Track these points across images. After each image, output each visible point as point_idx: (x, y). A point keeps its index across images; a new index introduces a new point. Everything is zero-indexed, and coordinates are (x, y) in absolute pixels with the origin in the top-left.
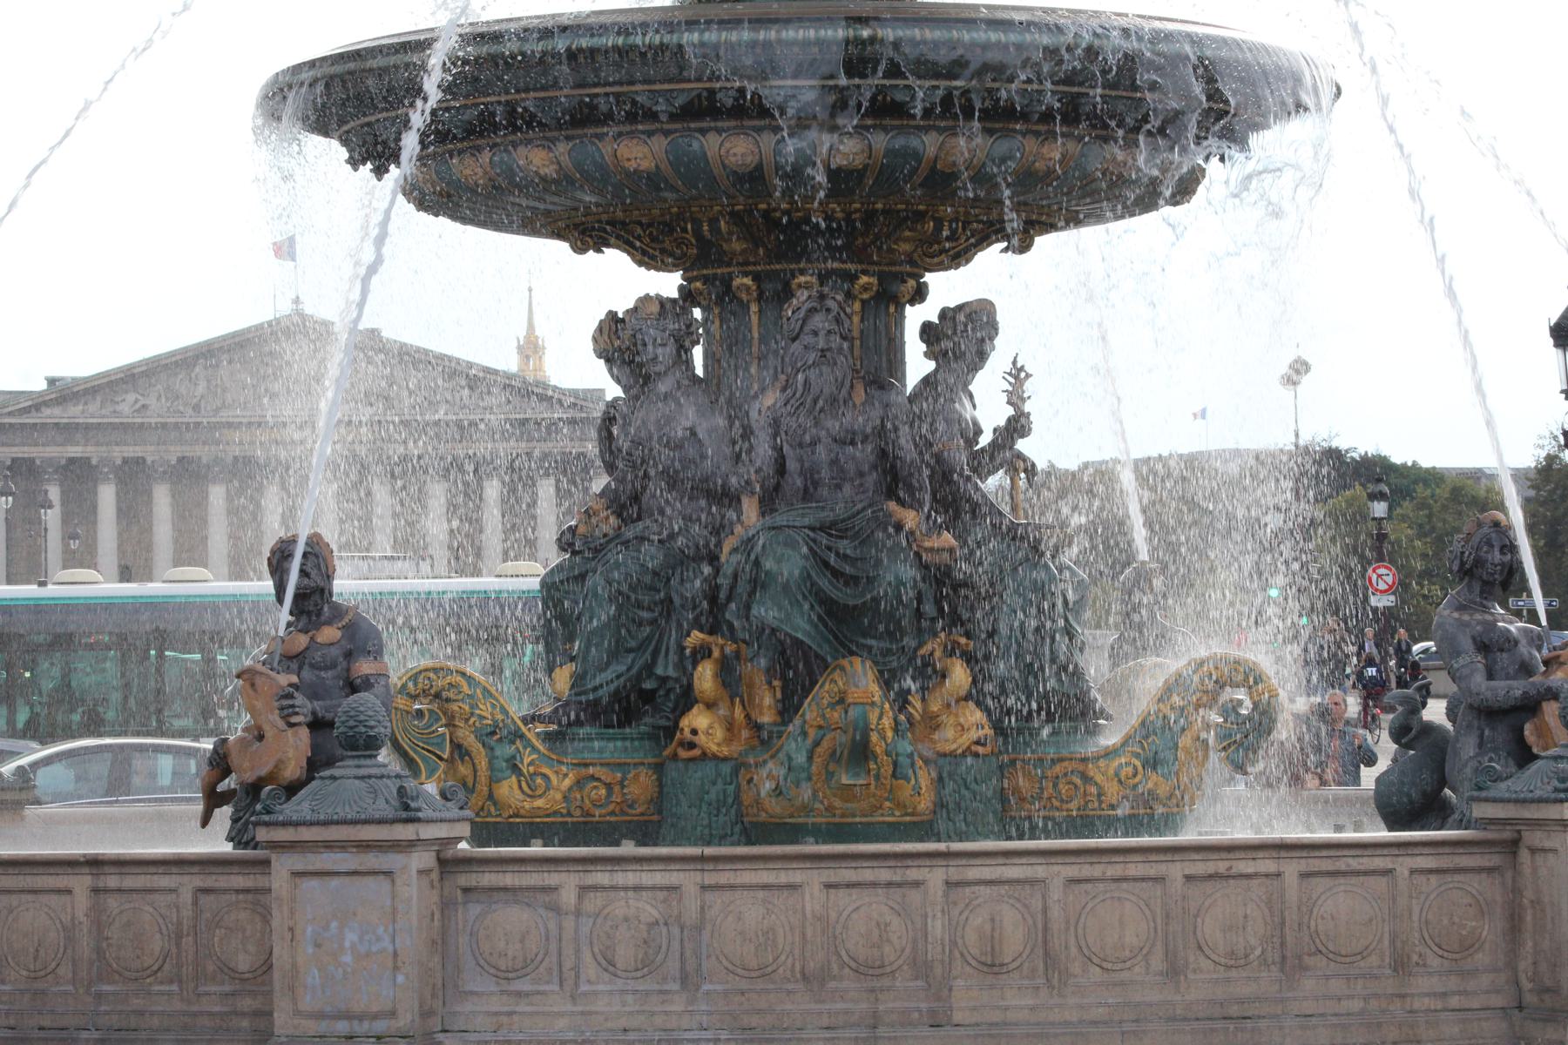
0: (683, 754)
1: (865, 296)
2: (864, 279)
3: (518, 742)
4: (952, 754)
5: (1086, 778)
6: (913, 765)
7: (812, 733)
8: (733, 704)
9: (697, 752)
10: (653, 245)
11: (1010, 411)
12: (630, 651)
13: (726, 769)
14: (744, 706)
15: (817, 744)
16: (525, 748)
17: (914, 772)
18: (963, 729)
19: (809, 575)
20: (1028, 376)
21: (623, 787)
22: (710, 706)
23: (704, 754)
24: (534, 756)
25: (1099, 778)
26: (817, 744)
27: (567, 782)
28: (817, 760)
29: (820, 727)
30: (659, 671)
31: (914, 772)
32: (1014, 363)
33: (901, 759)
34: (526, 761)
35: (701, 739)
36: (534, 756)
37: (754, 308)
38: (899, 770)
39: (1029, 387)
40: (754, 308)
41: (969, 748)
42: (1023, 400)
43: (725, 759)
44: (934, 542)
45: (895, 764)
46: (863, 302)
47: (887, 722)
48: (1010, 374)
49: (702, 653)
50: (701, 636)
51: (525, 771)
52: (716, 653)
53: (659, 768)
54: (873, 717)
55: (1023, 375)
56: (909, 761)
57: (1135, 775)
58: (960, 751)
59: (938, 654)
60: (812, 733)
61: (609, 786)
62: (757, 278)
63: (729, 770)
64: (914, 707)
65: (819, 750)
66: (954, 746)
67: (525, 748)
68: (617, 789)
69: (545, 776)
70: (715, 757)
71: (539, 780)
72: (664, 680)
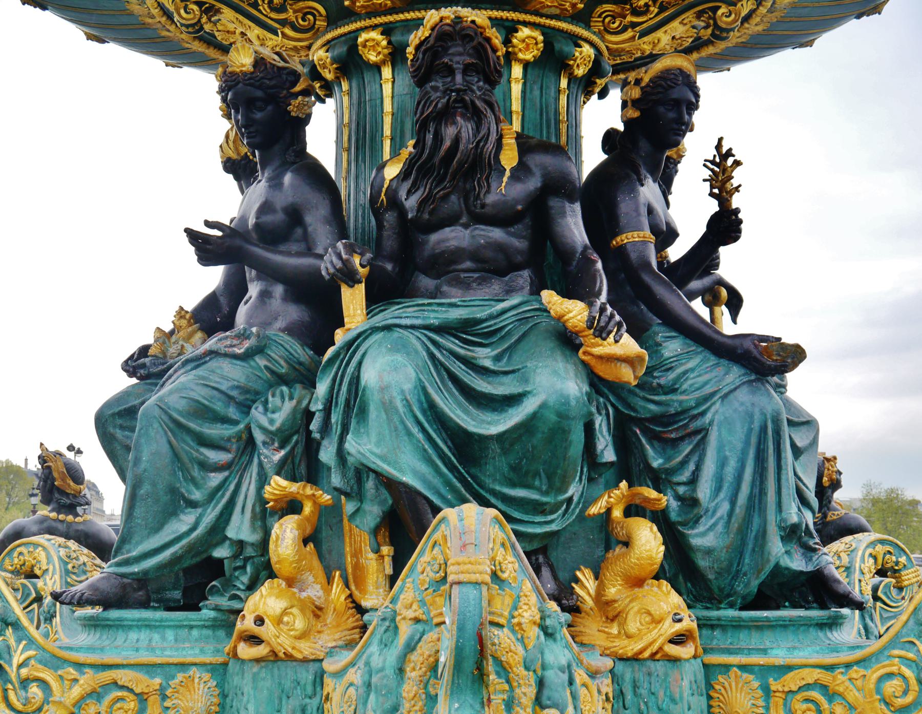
0: (246, 651)
1: (529, 56)
2: (525, 32)
3: (9, 631)
4: (635, 659)
5: (831, 694)
6: (571, 682)
7: (406, 630)
8: (330, 580)
9: (261, 651)
10: (273, 15)
11: (713, 206)
12: (193, 504)
13: (306, 675)
14: (347, 586)
15: (410, 647)
16: (19, 641)
17: (574, 697)
18: (657, 621)
19: (424, 389)
20: (737, 163)
21: (164, 697)
22: (291, 582)
23: (274, 653)
24: (31, 653)
25: (853, 695)
26: (410, 647)
27: (76, 691)
28: (413, 674)
29: (417, 620)
30: (231, 532)
31: (574, 697)
32: (719, 147)
33: (550, 675)
34: (17, 659)
35: (268, 631)
36: (31, 653)
37: (387, 72)
38: (546, 693)
39: (738, 177)
40: (387, 72)
41: (661, 649)
42: (731, 193)
43: (305, 661)
44: (607, 347)
45: (541, 684)
46: (526, 65)
47: (528, 613)
48: (713, 162)
49: (292, 506)
50: (283, 483)
51: (13, 675)
52: (308, 509)
53: (220, 670)
54: (502, 606)
55: (730, 161)
56: (565, 677)
57: (905, 692)
58: (646, 654)
59: (617, 513)
60: (406, 630)
61: (142, 698)
62: (387, 30)
63: (311, 677)
64: (583, 587)
65: (414, 657)
66: (638, 647)
67: (19, 641)
68: (154, 699)
69: (43, 683)
70: (289, 657)
71: (35, 690)
72: (240, 545)
